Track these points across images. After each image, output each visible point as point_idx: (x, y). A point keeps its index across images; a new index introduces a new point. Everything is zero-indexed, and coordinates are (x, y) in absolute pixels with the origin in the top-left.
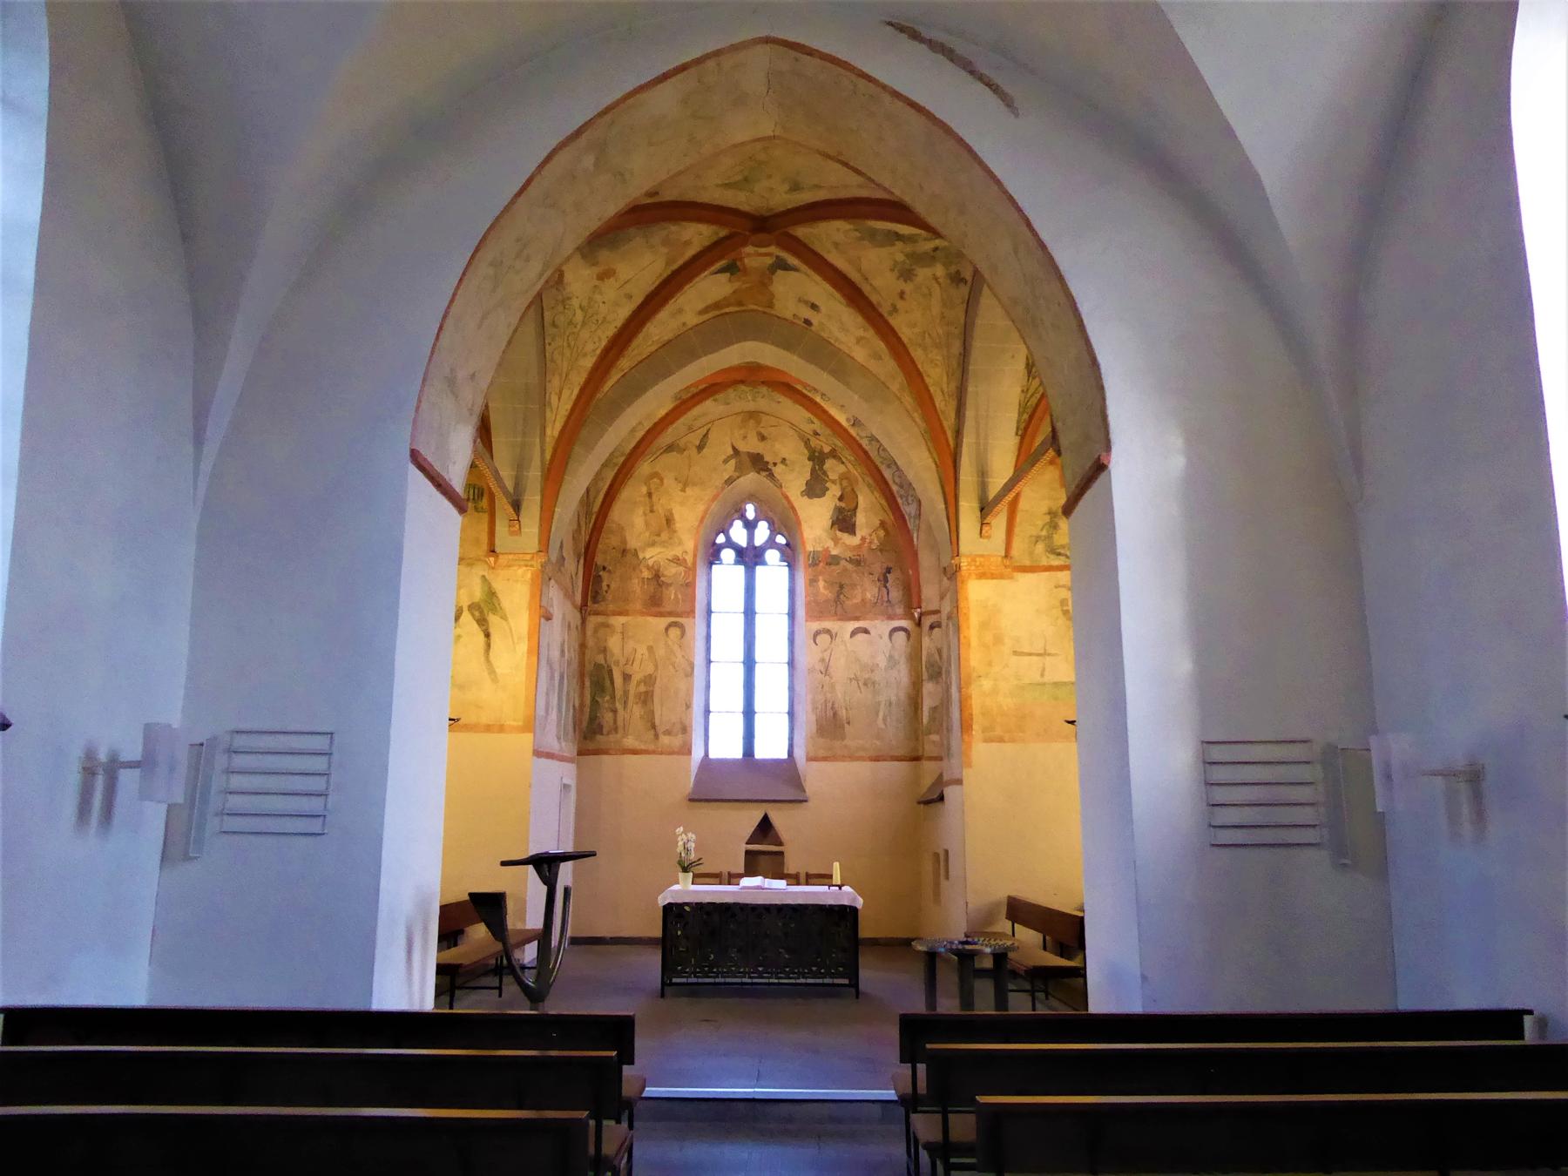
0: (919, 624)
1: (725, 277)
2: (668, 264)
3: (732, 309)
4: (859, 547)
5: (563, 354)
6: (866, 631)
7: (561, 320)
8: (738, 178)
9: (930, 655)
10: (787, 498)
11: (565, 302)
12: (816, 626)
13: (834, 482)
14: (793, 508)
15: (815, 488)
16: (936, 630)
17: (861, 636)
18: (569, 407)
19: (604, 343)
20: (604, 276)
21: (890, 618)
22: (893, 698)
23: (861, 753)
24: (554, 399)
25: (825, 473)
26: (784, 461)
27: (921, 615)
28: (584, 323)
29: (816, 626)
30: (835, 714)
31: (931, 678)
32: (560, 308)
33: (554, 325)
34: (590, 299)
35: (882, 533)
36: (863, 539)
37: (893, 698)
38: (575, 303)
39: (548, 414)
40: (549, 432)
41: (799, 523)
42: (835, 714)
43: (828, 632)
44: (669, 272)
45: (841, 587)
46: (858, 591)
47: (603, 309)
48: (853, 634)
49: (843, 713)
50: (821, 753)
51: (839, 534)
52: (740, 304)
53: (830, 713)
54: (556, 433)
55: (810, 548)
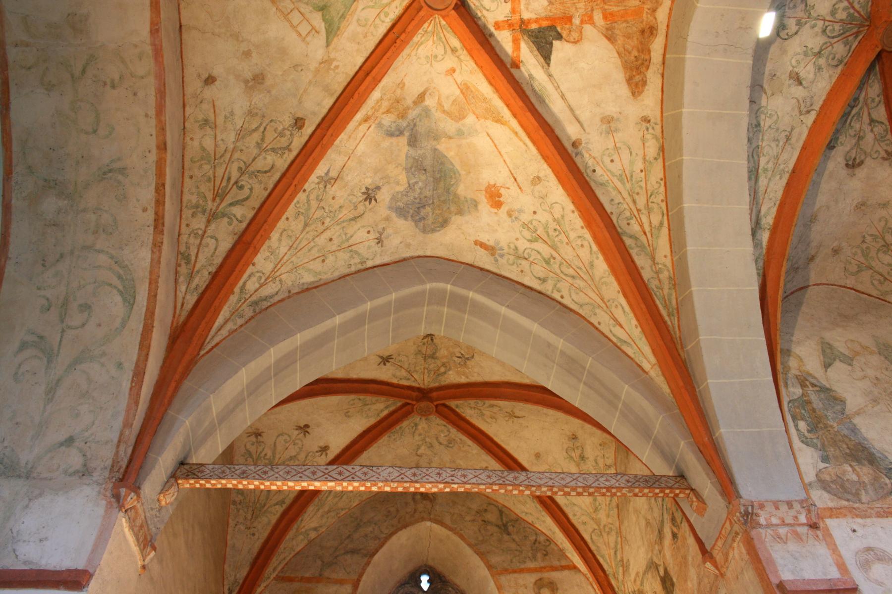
1: (560, 50)
2: (499, 120)
3: (657, 46)
5: (579, 289)
7: (539, 271)
8: (317, 20)
11: (520, 257)
18: (634, 322)
19: (588, 235)
20: (495, 197)
24: (618, 331)
28: (554, 247)
32: (524, 262)
33: (543, 280)
34: (525, 225)
38: (523, 245)
39: (630, 351)
40: (646, 366)
44: (514, 123)
47: (543, 217)
52: (652, 30)
54: (653, 360)
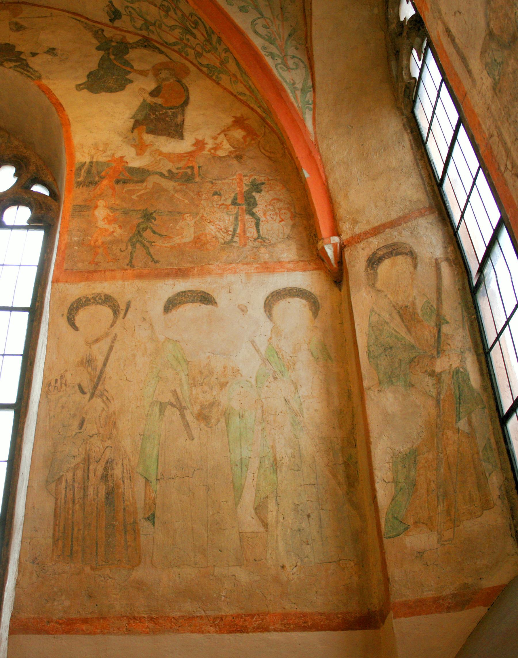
0: (338, 275)
4: (191, 154)
6: (206, 299)
9: (377, 328)
10: (47, 91)
12: (77, 290)
13: (143, 73)
14: (59, 106)
15: (106, 78)
16: (384, 267)
17: (190, 311)
21: (268, 268)
22: (284, 451)
23: (189, 607)
25: (127, 63)
26: (52, 51)
27: (341, 252)
29: (77, 290)
30: (111, 495)
31: (389, 379)
35: (238, 134)
36: (200, 145)
37: (284, 451)
41: (66, 123)
42: (111, 495)
43: (107, 300)
45: (148, 216)
46: (189, 220)
48: (171, 305)
49: (135, 493)
50: (61, 607)
51: (148, 138)
53: (97, 491)
55: (82, 157)
